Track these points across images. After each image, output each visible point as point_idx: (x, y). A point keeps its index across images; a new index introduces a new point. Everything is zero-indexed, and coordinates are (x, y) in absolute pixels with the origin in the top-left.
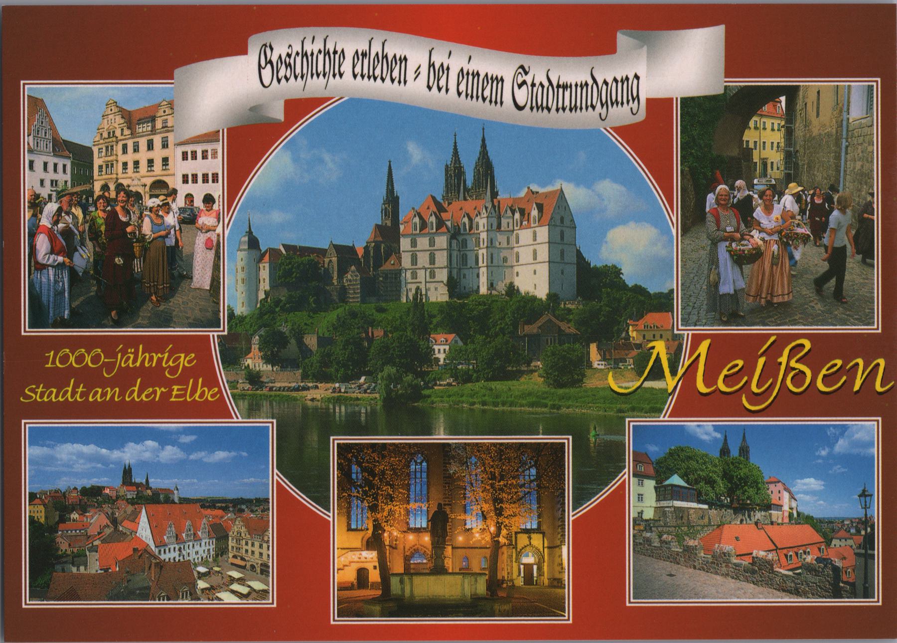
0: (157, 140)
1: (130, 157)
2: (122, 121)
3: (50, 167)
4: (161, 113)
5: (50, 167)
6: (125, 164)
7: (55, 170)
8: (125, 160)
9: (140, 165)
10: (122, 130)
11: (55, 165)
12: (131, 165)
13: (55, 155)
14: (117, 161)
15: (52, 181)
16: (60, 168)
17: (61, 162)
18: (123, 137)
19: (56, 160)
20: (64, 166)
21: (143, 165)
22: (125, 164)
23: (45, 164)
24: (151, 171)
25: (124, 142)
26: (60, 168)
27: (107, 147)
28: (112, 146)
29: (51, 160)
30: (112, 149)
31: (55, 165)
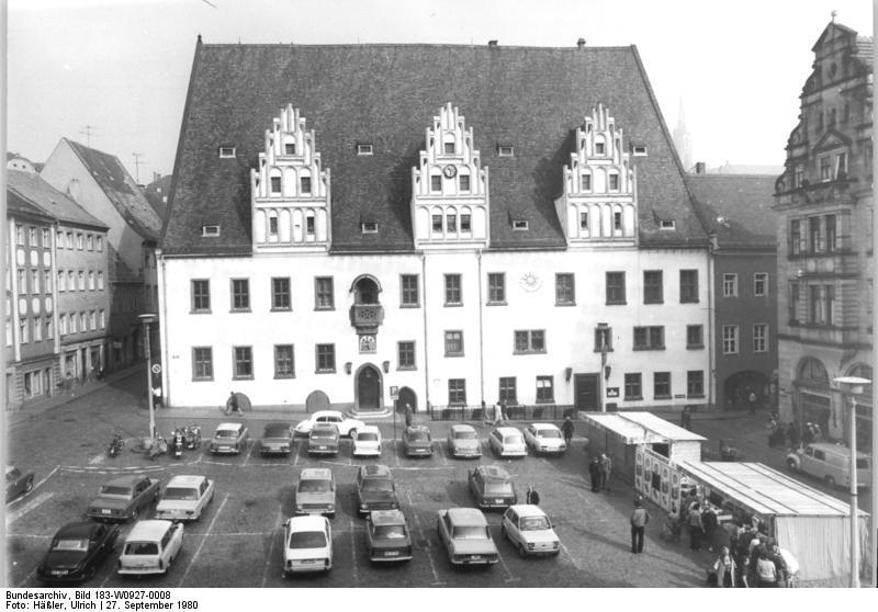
3: (634, 286)
5: (634, 286)
13: (646, 244)
15: (639, 333)
16: (671, 286)
19: (652, 260)
20: (688, 278)
26: (671, 286)
29: (635, 265)
31: (653, 280)
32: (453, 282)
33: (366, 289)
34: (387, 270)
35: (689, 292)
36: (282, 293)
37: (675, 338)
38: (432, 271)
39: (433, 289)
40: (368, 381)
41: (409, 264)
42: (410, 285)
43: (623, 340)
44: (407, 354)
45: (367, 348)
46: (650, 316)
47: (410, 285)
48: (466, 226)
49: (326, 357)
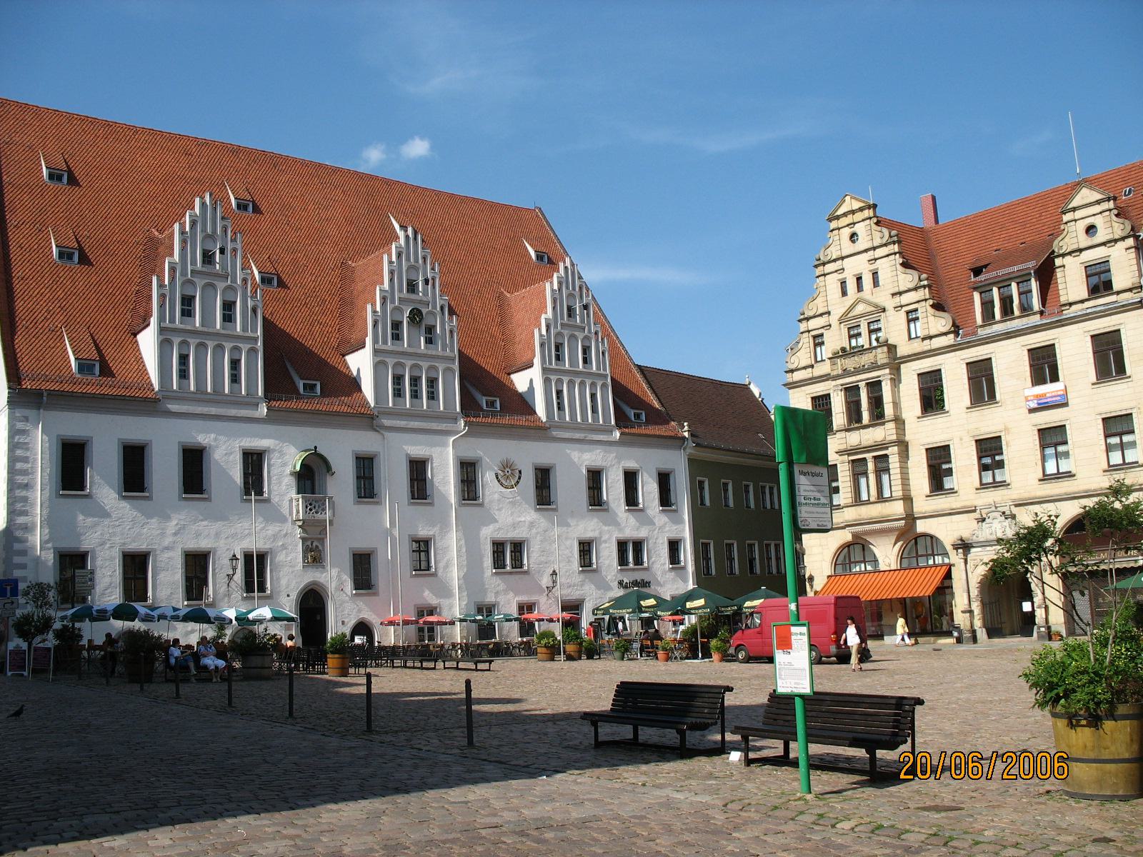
0: (1074, 348)
1: (959, 425)
2: (907, 279)
3: (613, 489)
4: (1074, 235)
5: (613, 489)
6: (939, 460)
7: (631, 499)
8: (937, 440)
9: (1009, 454)
10: (912, 318)
11: (630, 479)
12: (964, 461)
14: (903, 446)
16: (648, 489)
17: (647, 462)
18: (918, 347)
21: (964, 461)
22: (939, 460)
23: (595, 477)
24: (996, 485)
25: (926, 365)
27: (851, 391)
28: (875, 386)
30: (877, 402)
32: (418, 469)
33: (311, 476)
34: (341, 448)
35: (666, 499)
36: (194, 466)
37: (657, 558)
38: (394, 453)
39: (393, 478)
40: (312, 606)
41: (365, 441)
42: (366, 468)
43: (607, 556)
44: (363, 571)
45: (314, 556)
46: (630, 528)
47: (366, 468)
48: (432, 396)
49: (255, 569)
